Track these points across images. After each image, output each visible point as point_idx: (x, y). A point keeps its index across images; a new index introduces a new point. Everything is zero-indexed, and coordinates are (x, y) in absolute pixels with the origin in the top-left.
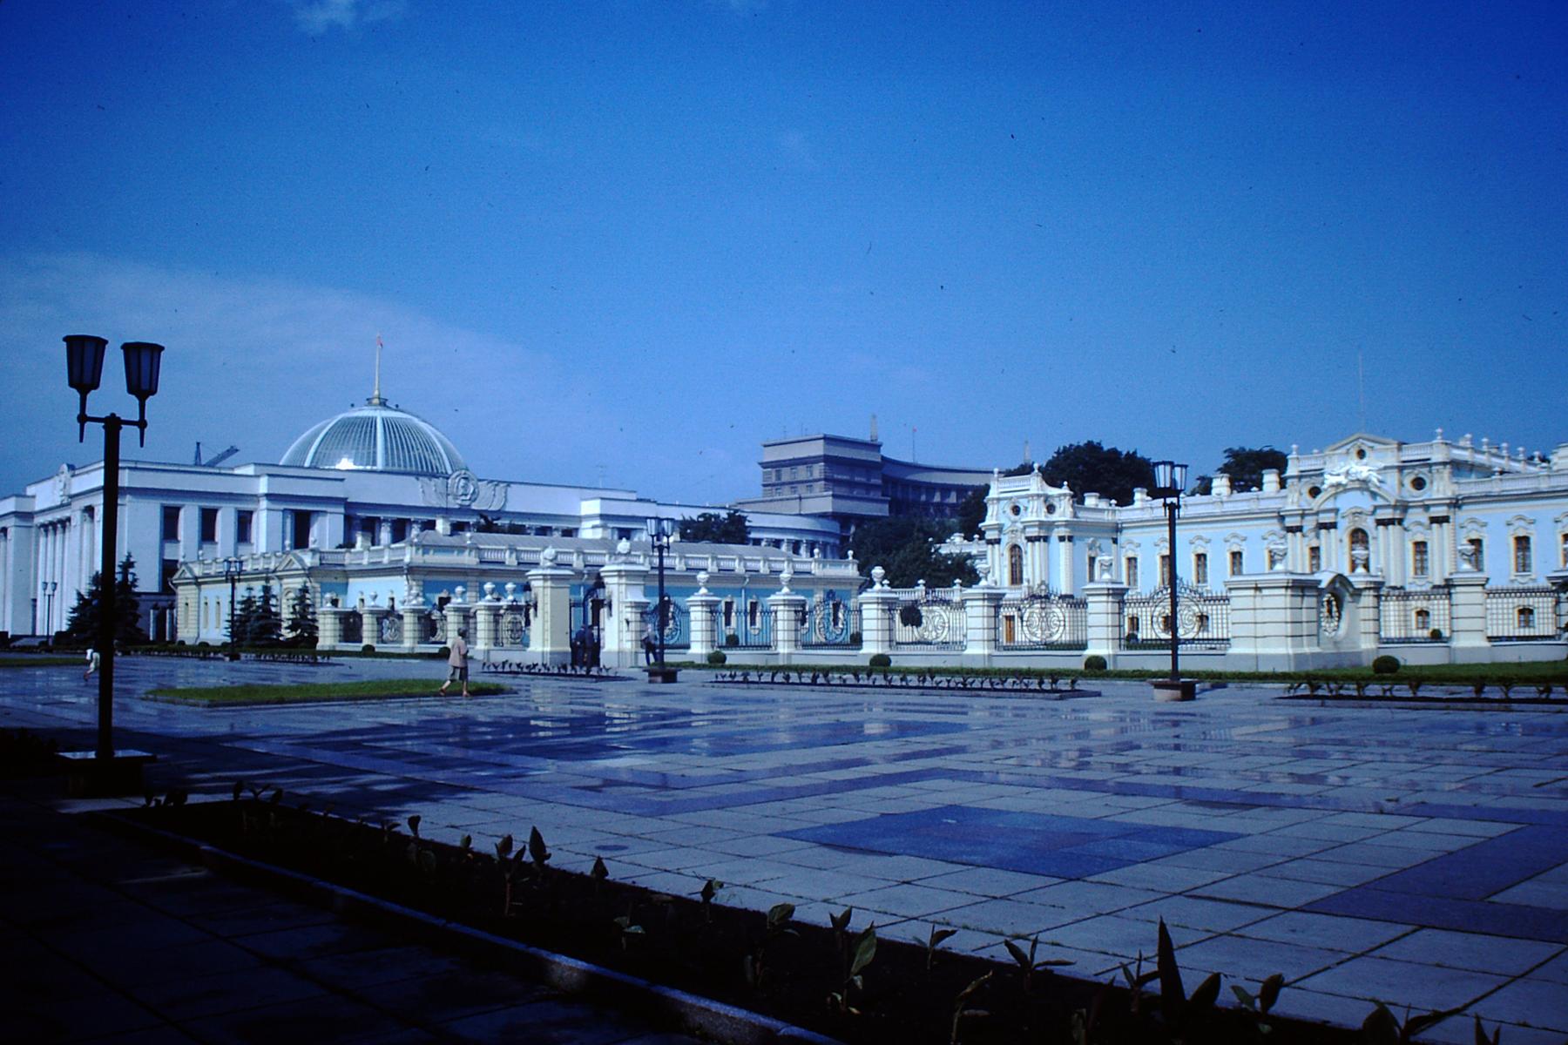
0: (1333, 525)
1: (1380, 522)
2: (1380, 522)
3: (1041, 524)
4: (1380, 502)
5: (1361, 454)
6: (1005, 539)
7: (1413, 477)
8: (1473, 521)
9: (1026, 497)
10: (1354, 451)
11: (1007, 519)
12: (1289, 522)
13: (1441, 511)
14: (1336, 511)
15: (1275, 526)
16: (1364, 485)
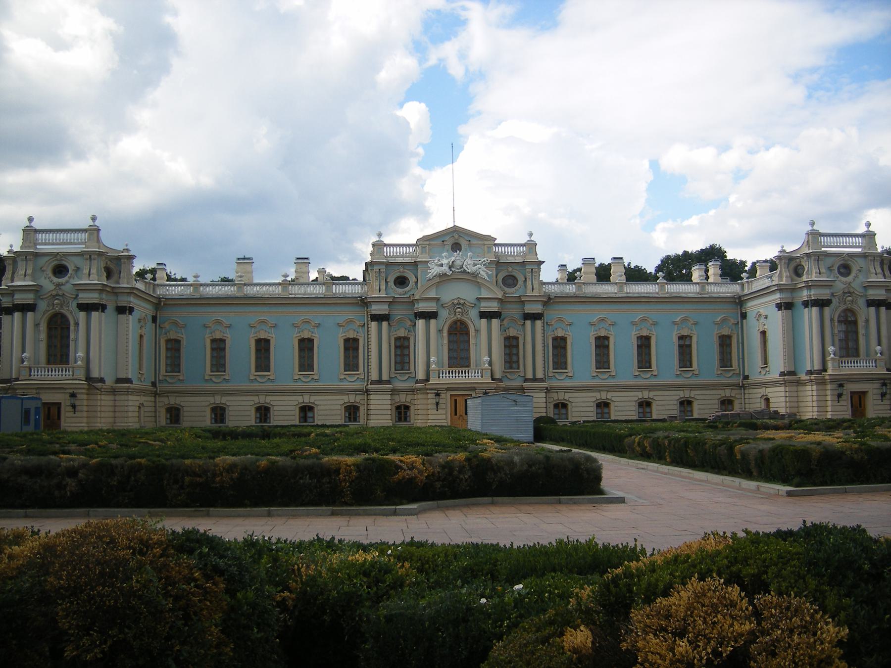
0: (433, 315)
1: (483, 315)
2: (483, 315)
3: (102, 289)
4: (485, 294)
5: (456, 247)
6: (42, 305)
7: (507, 274)
8: (560, 320)
9: (81, 254)
10: (449, 242)
11: (48, 283)
12: (376, 309)
13: (537, 309)
14: (438, 300)
15: (356, 315)
16: (473, 278)
